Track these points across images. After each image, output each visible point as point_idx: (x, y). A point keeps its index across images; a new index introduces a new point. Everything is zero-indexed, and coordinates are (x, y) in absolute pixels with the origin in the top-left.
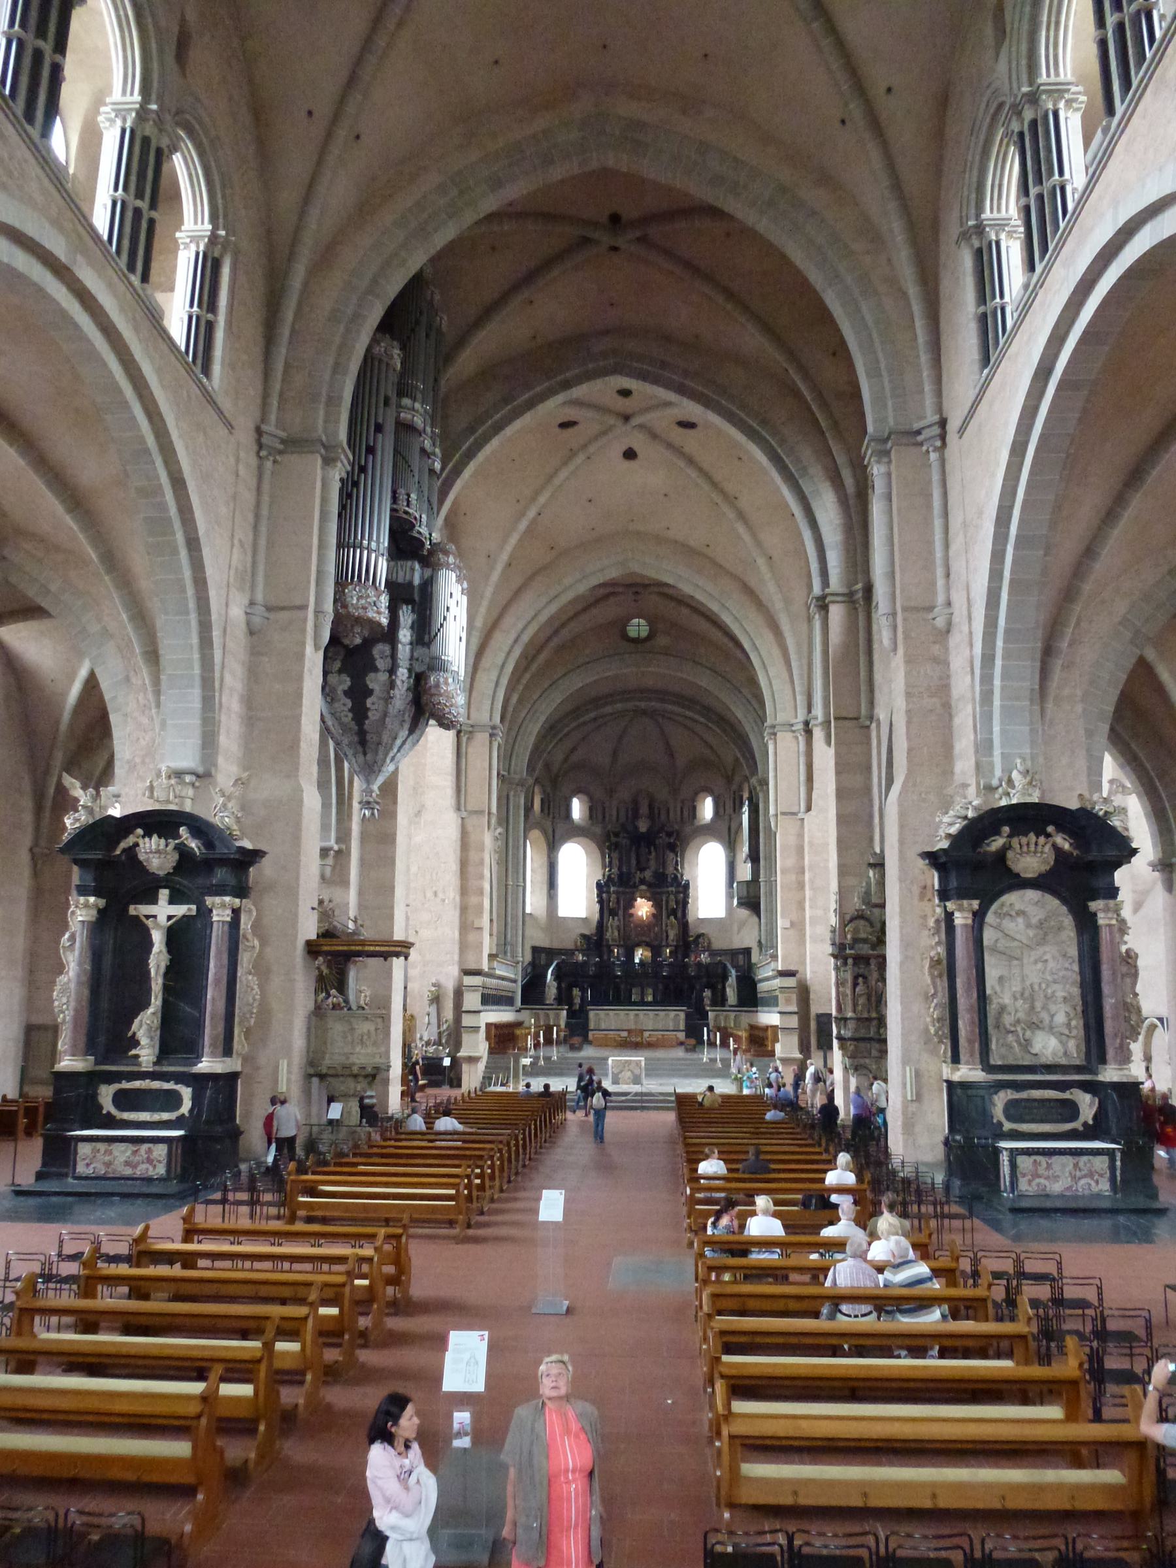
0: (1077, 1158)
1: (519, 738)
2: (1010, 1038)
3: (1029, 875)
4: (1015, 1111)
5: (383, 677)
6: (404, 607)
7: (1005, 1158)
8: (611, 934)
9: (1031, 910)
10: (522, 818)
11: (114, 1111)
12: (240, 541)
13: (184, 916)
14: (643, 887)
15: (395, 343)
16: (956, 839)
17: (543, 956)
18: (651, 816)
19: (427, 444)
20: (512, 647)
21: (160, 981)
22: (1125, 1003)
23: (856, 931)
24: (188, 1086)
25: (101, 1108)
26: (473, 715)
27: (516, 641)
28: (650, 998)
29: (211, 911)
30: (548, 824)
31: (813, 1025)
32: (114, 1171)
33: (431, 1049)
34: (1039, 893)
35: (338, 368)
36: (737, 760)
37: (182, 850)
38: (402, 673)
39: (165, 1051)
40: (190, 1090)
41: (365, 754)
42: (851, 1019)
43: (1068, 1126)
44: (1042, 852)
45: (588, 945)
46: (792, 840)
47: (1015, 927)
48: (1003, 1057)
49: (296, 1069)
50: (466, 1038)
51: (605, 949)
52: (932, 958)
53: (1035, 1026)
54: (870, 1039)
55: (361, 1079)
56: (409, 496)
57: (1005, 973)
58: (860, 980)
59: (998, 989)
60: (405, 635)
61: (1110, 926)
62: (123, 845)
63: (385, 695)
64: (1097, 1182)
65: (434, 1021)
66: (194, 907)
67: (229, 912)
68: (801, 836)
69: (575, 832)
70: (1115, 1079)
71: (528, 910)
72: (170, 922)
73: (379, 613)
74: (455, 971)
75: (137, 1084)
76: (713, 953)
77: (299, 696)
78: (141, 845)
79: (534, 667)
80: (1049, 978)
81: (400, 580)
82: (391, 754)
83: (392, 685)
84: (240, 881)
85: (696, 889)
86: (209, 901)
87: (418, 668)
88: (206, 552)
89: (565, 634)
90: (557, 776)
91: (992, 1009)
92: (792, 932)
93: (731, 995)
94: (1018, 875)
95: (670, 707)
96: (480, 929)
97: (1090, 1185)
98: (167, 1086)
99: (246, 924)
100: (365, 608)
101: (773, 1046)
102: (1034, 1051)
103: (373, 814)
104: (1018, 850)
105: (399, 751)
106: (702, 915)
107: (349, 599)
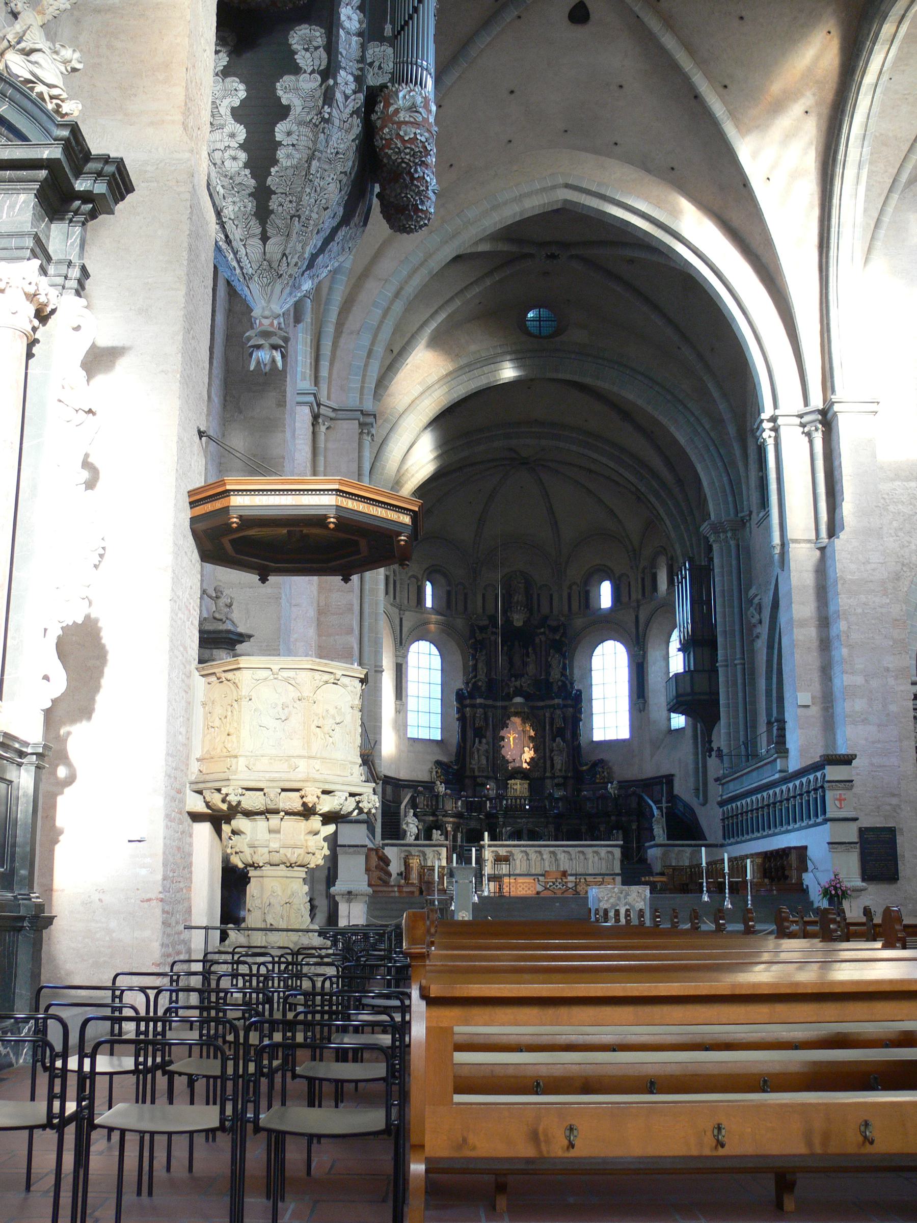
5: (309, 83)
8: (478, 762)
14: (518, 700)
20: (392, 302)
26: (332, 396)
27: (397, 295)
38: (345, 79)
55: (316, 822)
63: (312, 116)
76: (624, 785)
83: (328, 97)
85: (590, 700)
87: (372, 80)
93: (659, 831)
101: (800, 879)
106: (598, 736)
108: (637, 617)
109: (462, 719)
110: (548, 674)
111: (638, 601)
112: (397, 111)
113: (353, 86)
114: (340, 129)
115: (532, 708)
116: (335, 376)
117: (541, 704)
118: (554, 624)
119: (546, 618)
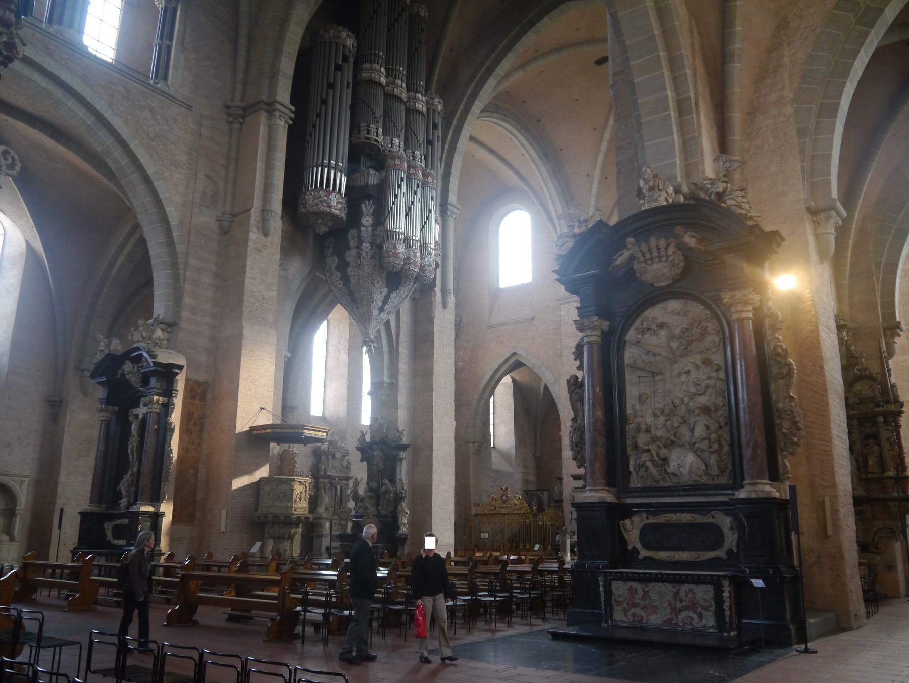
6: (367, 202)
9: (672, 320)
12: (208, 177)
15: (341, 28)
19: (401, 89)
25: (105, 536)
35: (278, 52)
38: (366, 246)
43: (710, 555)
44: (667, 256)
47: (657, 341)
56: (368, 126)
60: (367, 221)
62: (119, 372)
64: (701, 617)
73: (330, 206)
77: (245, 266)
81: (362, 184)
83: (359, 256)
87: (378, 242)
88: (157, 184)
97: (692, 619)
100: (316, 205)
104: (642, 259)
107: (307, 202)
113: (370, 248)
114: (367, 265)
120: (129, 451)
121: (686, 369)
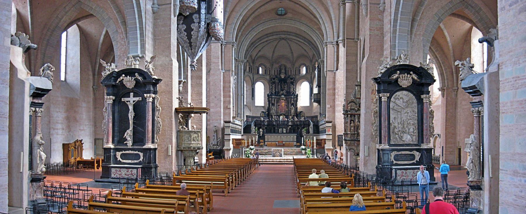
0: (414, 170)
1: (241, 47)
2: (397, 136)
3: (404, 87)
4: (397, 158)
5: (197, 25)
7: (394, 171)
8: (273, 111)
10: (243, 73)
11: (121, 160)
13: (138, 101)
14: (283, 96)
16: (383, 74)
17: (250, 119)
18: (285, 73)
21: (132, 121)
22: (430, 126)
23: (351, 106)
24: (141, 152)
25: (117, 159)
26: (226, 39)
28: (285, 132)
29: (146, 99)
30: (251, 76)
31: (337, 139)
32: (122, 176)
33: (215, 147)
34: (407, 92)
36: (314, 55)
37: (136, 80)
39: (134, 143)
40: (142, 154)
41: (191, 49)
42: (349, 134)
43: (412, 162)
45: (265, 114)
46: (332, 80)
48: (394, 142)
49: (174, 148)
50: (226, 143)
51: (270, 116)
52: (374, 111)
53: (404, 132)
54: (355, 140)
57: (396, 117)
58: (352, 121)
59: (394, 121)
61: (427, 102)
65: (216, 138)
66: (141, 98)
67: (151, 98)
68: (334, 78)
69: (260, 78)
70: (426, 148)
71: (245, 104)
72: (134, 103)
74: (222, 122)
75: (127, 152)
78: (124, 80)
79: (246, 24)
80: (409, 118)
82: (200, 49)
84: (154, 89)
86: (145, 95)
87: (208, 22)
89: (256, 13)
90: (254, 60)
91: (392, 127)
92: (331, 109)
93: (311, 130)
94: (401, 86)
95: (291, 37)
96: (230, 108)
98: (135, 152)
99: (157, 103)
101: (324, 145)
102: (403, 140)
103: (195, 69)
104: (402, 79)
105: (202, 48)
108: (311, 76)
109: (269, 101)
110: (290, 90)
111: (311, 73)
112: (212, 27)
115: (286, 98)
116: (226, 35)
117: (288, 97)
118: (291, 77)
119: (289, 76)
120: (130, 119)
121: (408, 112)
